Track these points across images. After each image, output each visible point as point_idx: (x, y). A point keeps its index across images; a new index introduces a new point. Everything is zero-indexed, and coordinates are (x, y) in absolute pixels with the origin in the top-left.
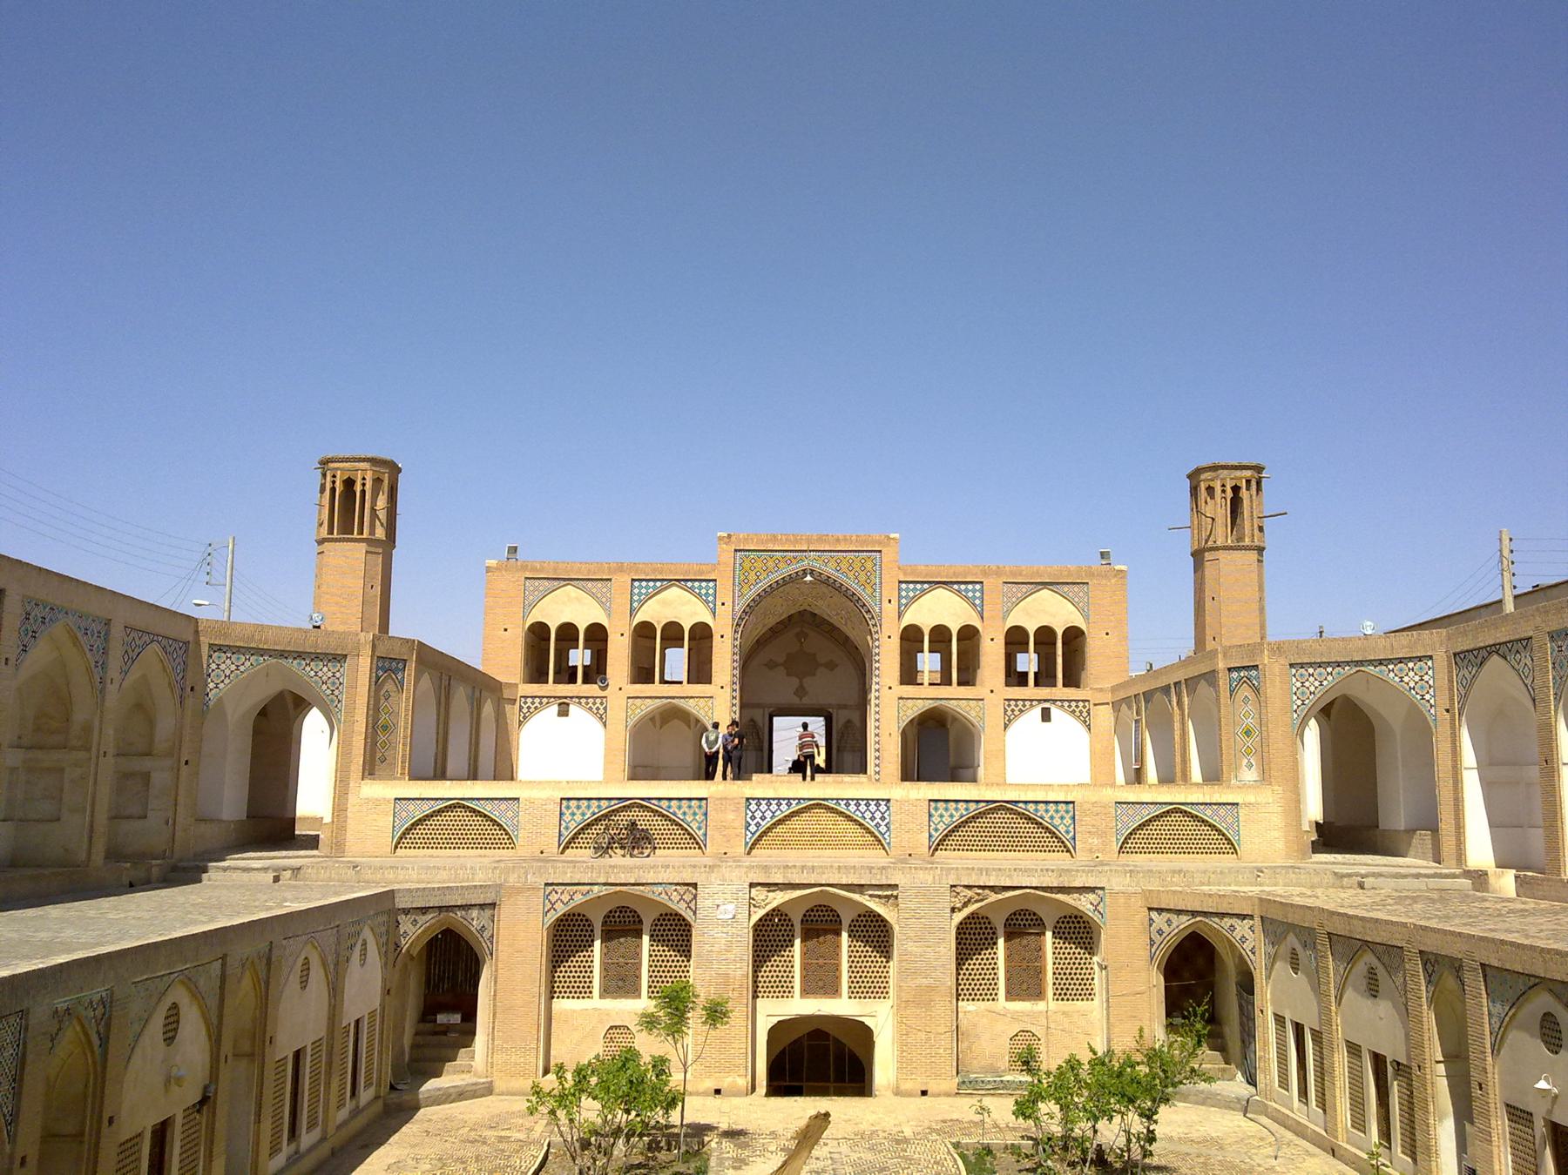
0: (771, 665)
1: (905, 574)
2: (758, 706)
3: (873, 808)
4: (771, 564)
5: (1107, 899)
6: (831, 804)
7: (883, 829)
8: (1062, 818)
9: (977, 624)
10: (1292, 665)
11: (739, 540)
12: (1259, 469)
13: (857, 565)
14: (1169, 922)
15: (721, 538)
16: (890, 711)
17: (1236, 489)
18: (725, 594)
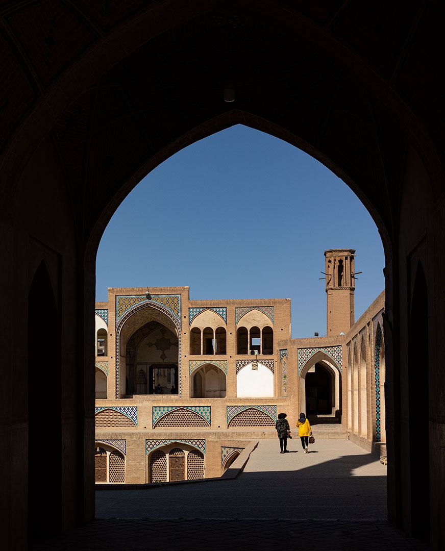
0: (150, 345)
1: (192, 305)
2: (146, 364)
3: (130, 410)
4: (132, 301)
5: (206, 443)
6: (114, 409)
7: (135, 419)
8: (206, 413)
9: (225, 327)
10: (298, 349)
11: (117, 291)
12: (353, 252)
13: (170, 301)
14: (227, 452)
15: (110, 290)
16: (188, 363)
17: (341, 261)
18: (112, 315)
